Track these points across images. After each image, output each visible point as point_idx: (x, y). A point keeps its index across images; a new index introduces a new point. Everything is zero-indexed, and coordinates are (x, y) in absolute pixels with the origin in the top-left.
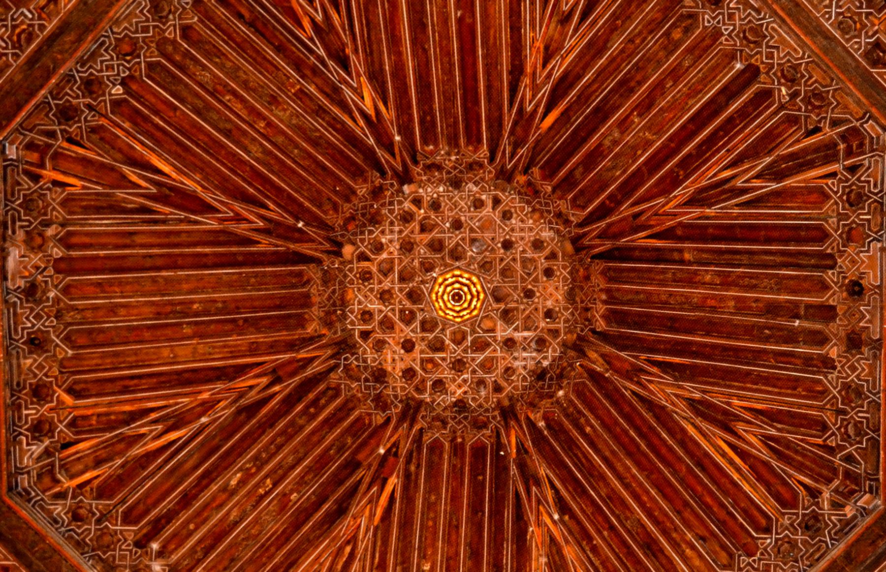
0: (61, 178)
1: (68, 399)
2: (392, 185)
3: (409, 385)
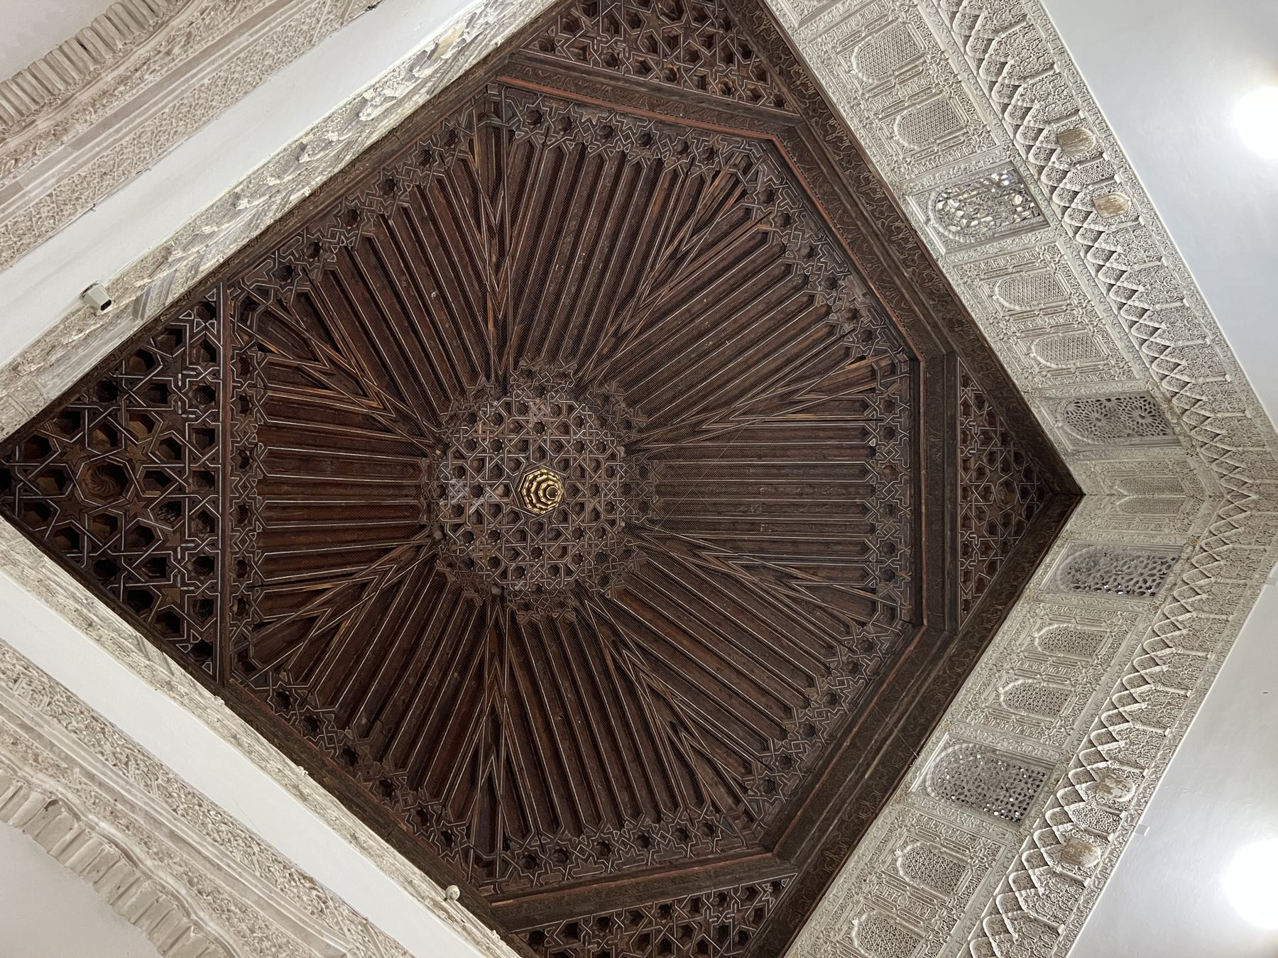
0: (863, 362)
1: (764, 227)
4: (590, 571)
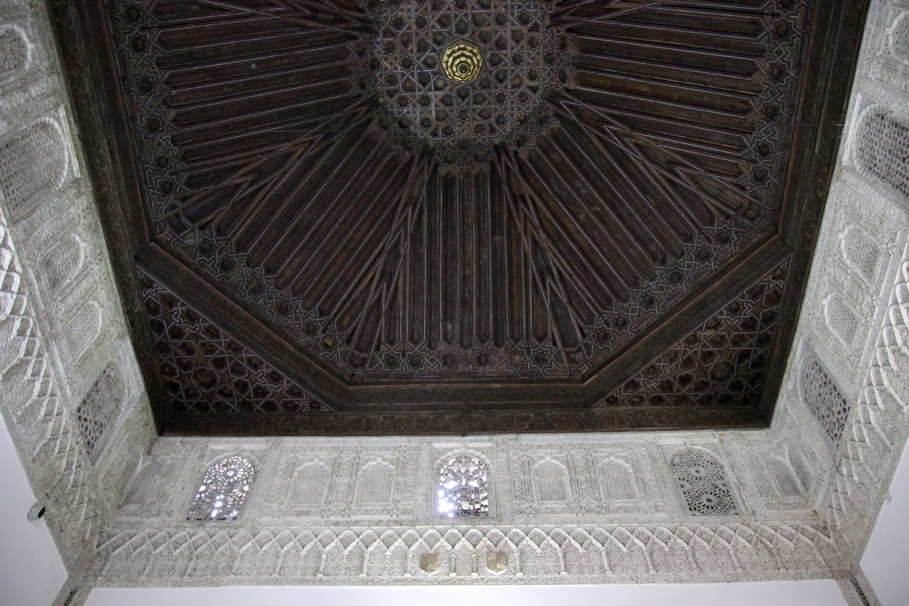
2: (550, 9)
3: (389, 24)
4: (549, 75)
